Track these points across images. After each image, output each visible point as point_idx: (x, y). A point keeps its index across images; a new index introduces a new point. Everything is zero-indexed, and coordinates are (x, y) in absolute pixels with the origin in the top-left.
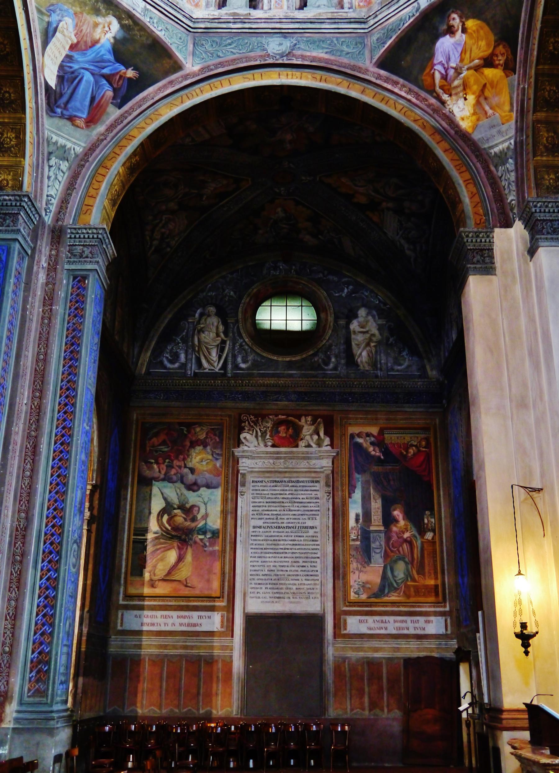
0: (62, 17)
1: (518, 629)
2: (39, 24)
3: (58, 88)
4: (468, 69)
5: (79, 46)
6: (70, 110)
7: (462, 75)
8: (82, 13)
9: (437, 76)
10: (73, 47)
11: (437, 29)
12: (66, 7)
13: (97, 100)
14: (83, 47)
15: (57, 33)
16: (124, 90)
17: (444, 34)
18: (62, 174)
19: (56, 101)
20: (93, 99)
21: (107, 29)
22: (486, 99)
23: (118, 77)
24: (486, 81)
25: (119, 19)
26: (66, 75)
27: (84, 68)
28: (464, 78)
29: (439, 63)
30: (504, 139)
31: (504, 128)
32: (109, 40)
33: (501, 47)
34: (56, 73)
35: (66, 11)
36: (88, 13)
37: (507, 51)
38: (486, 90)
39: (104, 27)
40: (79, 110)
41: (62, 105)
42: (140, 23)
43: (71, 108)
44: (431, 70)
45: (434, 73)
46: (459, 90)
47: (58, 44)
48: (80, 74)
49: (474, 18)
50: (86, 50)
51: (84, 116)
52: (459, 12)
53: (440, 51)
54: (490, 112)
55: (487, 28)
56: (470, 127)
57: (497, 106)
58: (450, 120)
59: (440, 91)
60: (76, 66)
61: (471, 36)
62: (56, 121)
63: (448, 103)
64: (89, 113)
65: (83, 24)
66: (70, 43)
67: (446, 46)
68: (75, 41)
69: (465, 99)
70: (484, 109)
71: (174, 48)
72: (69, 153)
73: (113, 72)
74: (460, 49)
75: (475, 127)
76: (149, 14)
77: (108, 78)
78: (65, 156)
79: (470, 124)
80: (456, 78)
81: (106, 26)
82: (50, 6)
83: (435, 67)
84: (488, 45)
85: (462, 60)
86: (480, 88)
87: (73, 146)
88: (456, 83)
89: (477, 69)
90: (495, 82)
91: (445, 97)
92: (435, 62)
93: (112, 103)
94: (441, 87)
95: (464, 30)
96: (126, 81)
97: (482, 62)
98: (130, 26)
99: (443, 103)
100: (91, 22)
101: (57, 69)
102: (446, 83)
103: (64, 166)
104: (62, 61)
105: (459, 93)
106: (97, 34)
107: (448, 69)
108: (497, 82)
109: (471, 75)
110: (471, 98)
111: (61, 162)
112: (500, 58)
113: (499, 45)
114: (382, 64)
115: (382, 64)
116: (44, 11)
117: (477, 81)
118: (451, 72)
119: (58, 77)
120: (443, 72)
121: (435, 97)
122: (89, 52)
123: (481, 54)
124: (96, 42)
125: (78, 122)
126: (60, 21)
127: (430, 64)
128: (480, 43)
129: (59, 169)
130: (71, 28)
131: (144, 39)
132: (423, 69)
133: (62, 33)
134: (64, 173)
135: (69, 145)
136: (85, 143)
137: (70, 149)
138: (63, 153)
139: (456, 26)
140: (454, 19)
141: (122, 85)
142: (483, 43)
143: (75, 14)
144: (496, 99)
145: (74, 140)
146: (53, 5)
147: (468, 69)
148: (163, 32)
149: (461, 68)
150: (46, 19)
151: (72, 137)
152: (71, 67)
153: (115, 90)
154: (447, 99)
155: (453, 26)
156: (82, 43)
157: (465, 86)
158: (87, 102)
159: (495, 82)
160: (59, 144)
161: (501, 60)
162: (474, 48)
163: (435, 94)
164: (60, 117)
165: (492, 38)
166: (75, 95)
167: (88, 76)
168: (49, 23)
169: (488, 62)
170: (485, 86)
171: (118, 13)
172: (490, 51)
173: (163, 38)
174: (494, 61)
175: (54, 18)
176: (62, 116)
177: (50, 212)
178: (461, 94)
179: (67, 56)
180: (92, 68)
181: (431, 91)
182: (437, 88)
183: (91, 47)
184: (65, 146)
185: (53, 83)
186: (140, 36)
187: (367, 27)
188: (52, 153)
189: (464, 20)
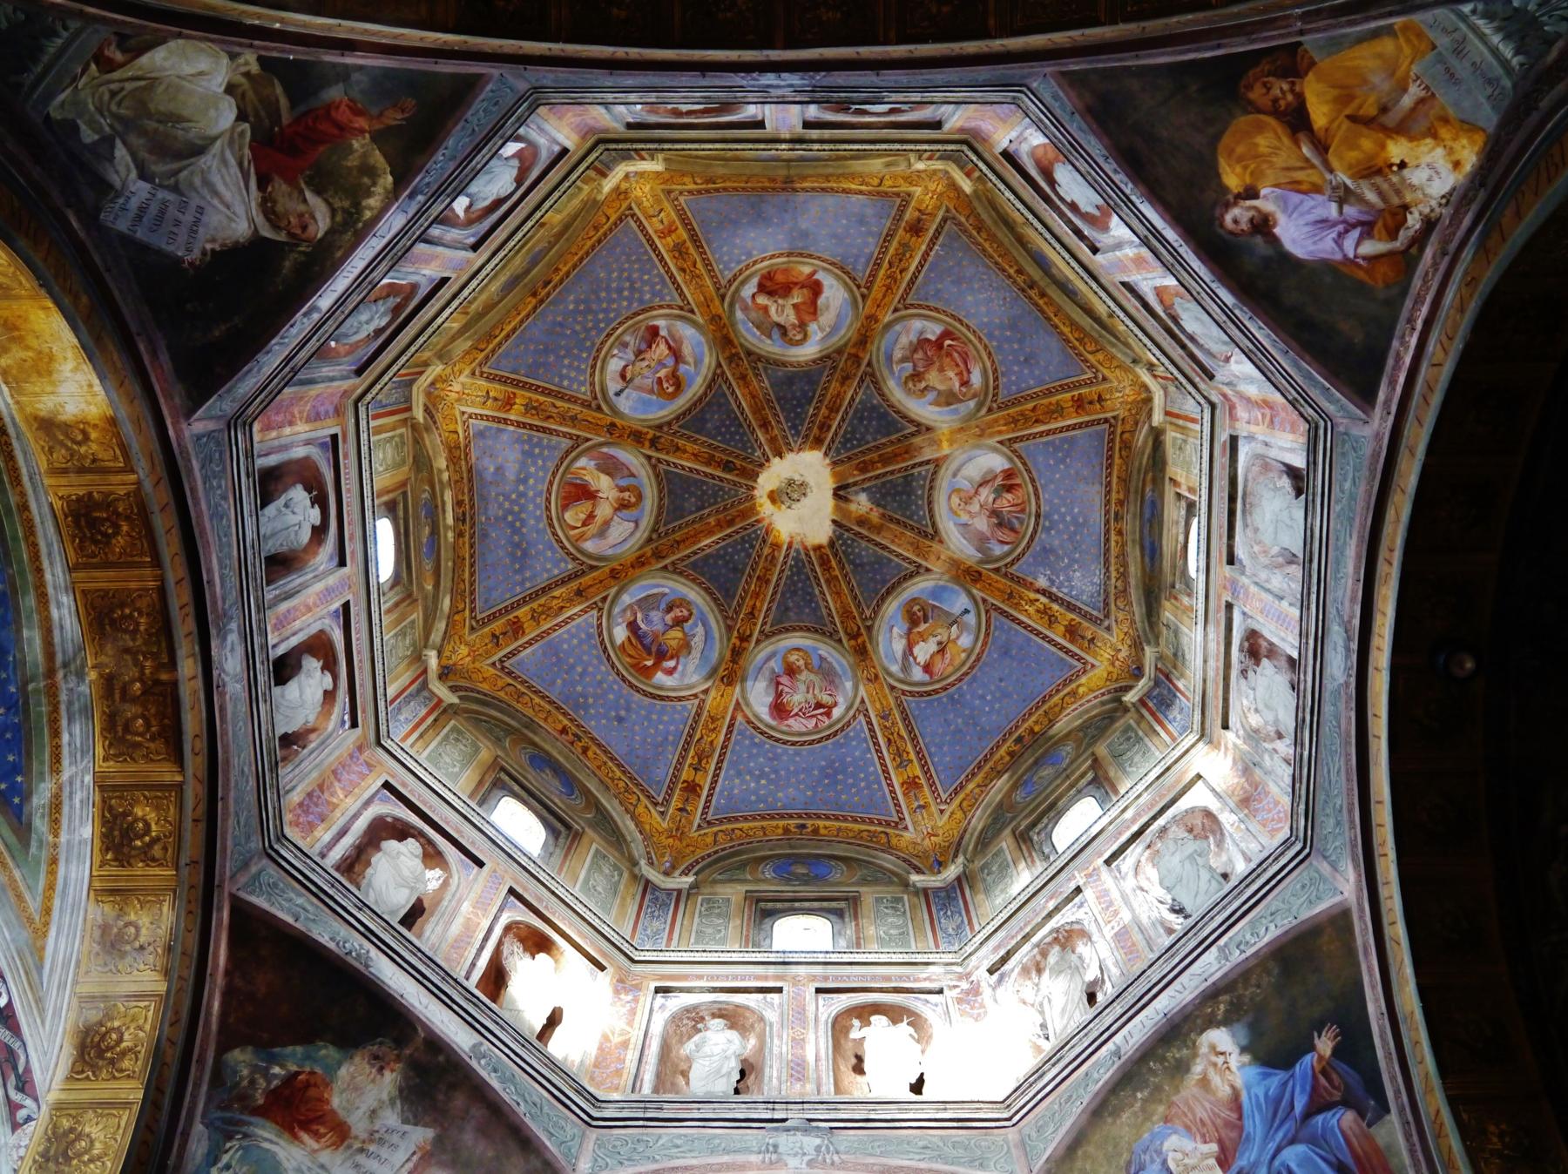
4: (1331, 171)
7: (1349, 182)
8: (1171, 1105)
9: (1370, 248)
17: (1274, 241)
21: (1220, 1060)
22: (1384, 110)
24: (1342, 118)
25: (1211, 1023)
28: (1351, 177)
29: (1340, 246)
30: (1471, 36)
31: (1443, 42)
32: (1243, 1065)
33: (1253, 95)
36: (1177, 1091)
37: (1256, 80)
38: (1361, 112)
39: (1215, 1065)
42: (1232, 976)
44: (1357, 265)
45: (1364, 258)
46: (1385, 186)
49: (1218, 176)
52: (1217, 212)
53: (1312, 248)
55: (1226, 139)
56: (1472, 142)
57: (1393, 74)
58: (1459, 200)
63: (1427, 210)
67: (1302, 230)
69: (1402, 165)
70: (1413, 110)
71: (1306, 914)
74: (1296, 198)
75: (1468, 126)
76: (1232, 946)
79: (1465, 142)
80: (1361, 200)
81: (1214, 1058)
83: (1351, 255)
84: (1260, 128)
85: (1316, 189)
86: (1365, 131)
88: (1371, 196)
89: (1322, 147)
90: (1336, 92)
91: (1414, 221)
92: (1338, 257)
94: (1392, 234)
96: (1342, 1067)
97: (1302, 136)
98: (1231, 1003)
99: (1429, 224)
100: (1195, 1090)
102: (1380, 224)
105: (1392, 185)
106: (1224, 1091)
107: (1345, 222)
108: (1333, 87)
109: (1341, 158)
110: (1396, 150)
112: (1276, 92)
113: (1250, 102)
114: (1365, 395)
115: (1365, 395)
118: (1351, 211)
120: (1355, 233)
121: (1422, 250)
123: (1286, 141)
124: (1235, 1102)
127: (1344, 269)
128: (1263, 150)
131: (1266, 979)
132: (1361, 288)
139: (1251, 213)
140: (1236, 221)
142: (1263, 142)
143: (1166, 1120)
144: (1376, 79)
147: (1331, 171)
148: (1272, 927)
149: (1334, 189)
154: (1416, 215)
155: (1251, 220)
157: (1373, 170)
159: (1336, 92)
161: (1280, 87)
162: (1280, 161)
163: (1414, 251)
165: (1243, 121)
169: (1297, 121)
170: (1353, 118)
171: (1199, 1021)
172: (1271, 121)
173: (1279, 932)
174: (1288, 105)
178: (1395, 179)
181: (1405, 261)
182: (1397, 245)
186: (1258, 986)
187: (1322, 423)
189: (1231, 198)
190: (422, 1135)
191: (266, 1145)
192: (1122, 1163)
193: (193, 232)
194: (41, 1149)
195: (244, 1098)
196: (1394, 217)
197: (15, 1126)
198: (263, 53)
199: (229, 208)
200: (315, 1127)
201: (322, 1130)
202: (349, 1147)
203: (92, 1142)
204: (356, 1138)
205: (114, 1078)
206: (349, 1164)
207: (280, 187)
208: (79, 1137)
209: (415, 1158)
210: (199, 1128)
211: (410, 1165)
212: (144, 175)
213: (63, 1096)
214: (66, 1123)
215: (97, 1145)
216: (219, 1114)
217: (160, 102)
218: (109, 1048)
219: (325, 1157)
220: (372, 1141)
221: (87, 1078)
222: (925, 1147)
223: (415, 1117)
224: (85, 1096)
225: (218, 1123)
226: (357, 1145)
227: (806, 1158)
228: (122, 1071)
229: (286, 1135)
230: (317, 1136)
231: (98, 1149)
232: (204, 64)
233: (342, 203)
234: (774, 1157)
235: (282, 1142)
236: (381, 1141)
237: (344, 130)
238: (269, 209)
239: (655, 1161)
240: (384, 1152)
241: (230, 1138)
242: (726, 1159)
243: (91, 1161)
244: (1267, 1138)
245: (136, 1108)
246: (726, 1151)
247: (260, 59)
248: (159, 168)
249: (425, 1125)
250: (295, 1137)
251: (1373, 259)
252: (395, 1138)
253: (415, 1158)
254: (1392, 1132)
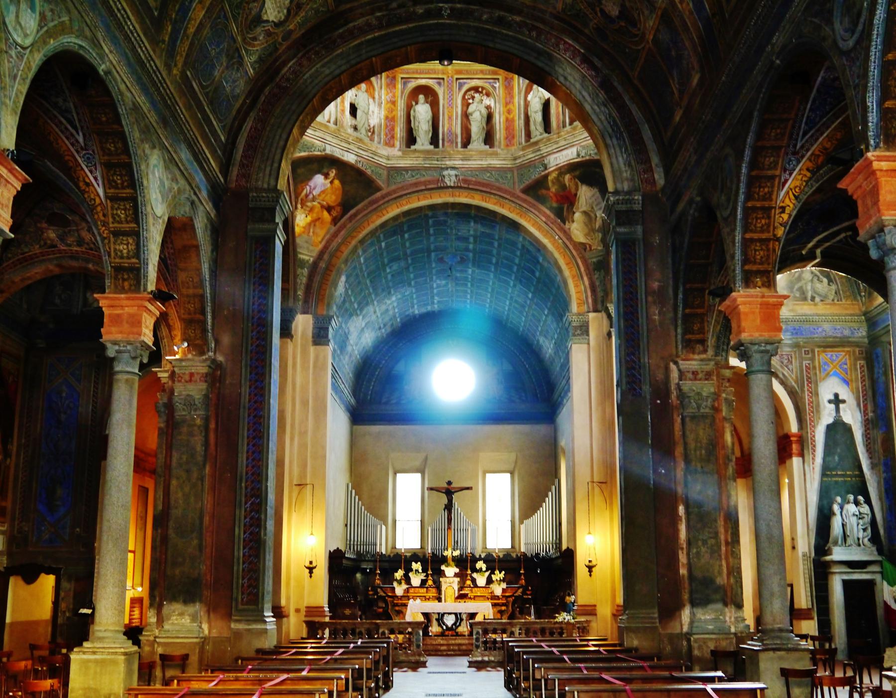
1: (308, 564)
9: (305, 192)
11: (323, 168)
31: (311, 248)
54: (311, 234)
55: (341, 191)
59: (300, 201)
61: (332, 188)
67: (319, 180)
74: (323, 189)
75: (300, 235)
84: (335, 201)
85: (319, 195)
88: (309, 204)
89: (322, 207)
91: (299, 206)
94: (302, 200)
95: (331, 182)
99: (296, 208)
110: (309, 219)
117: (318, 213)
118: (311, 196)
142: (334, 197)
157: (311, 210)
161: (334, 213)
165: (339, 200)
169: (329, 209)
193: (593, 196)
196: (303, 205)
198: (562, 224)
199: (585, 194)
207: (573, 191)
212: (596, 217)
217: (586, 231)
232: (575, 232)
233: (561, 179)
237: (555, 195)
238: (577, 189)
247: (565, 224)
248: (593, 215)
251: (303, 190)
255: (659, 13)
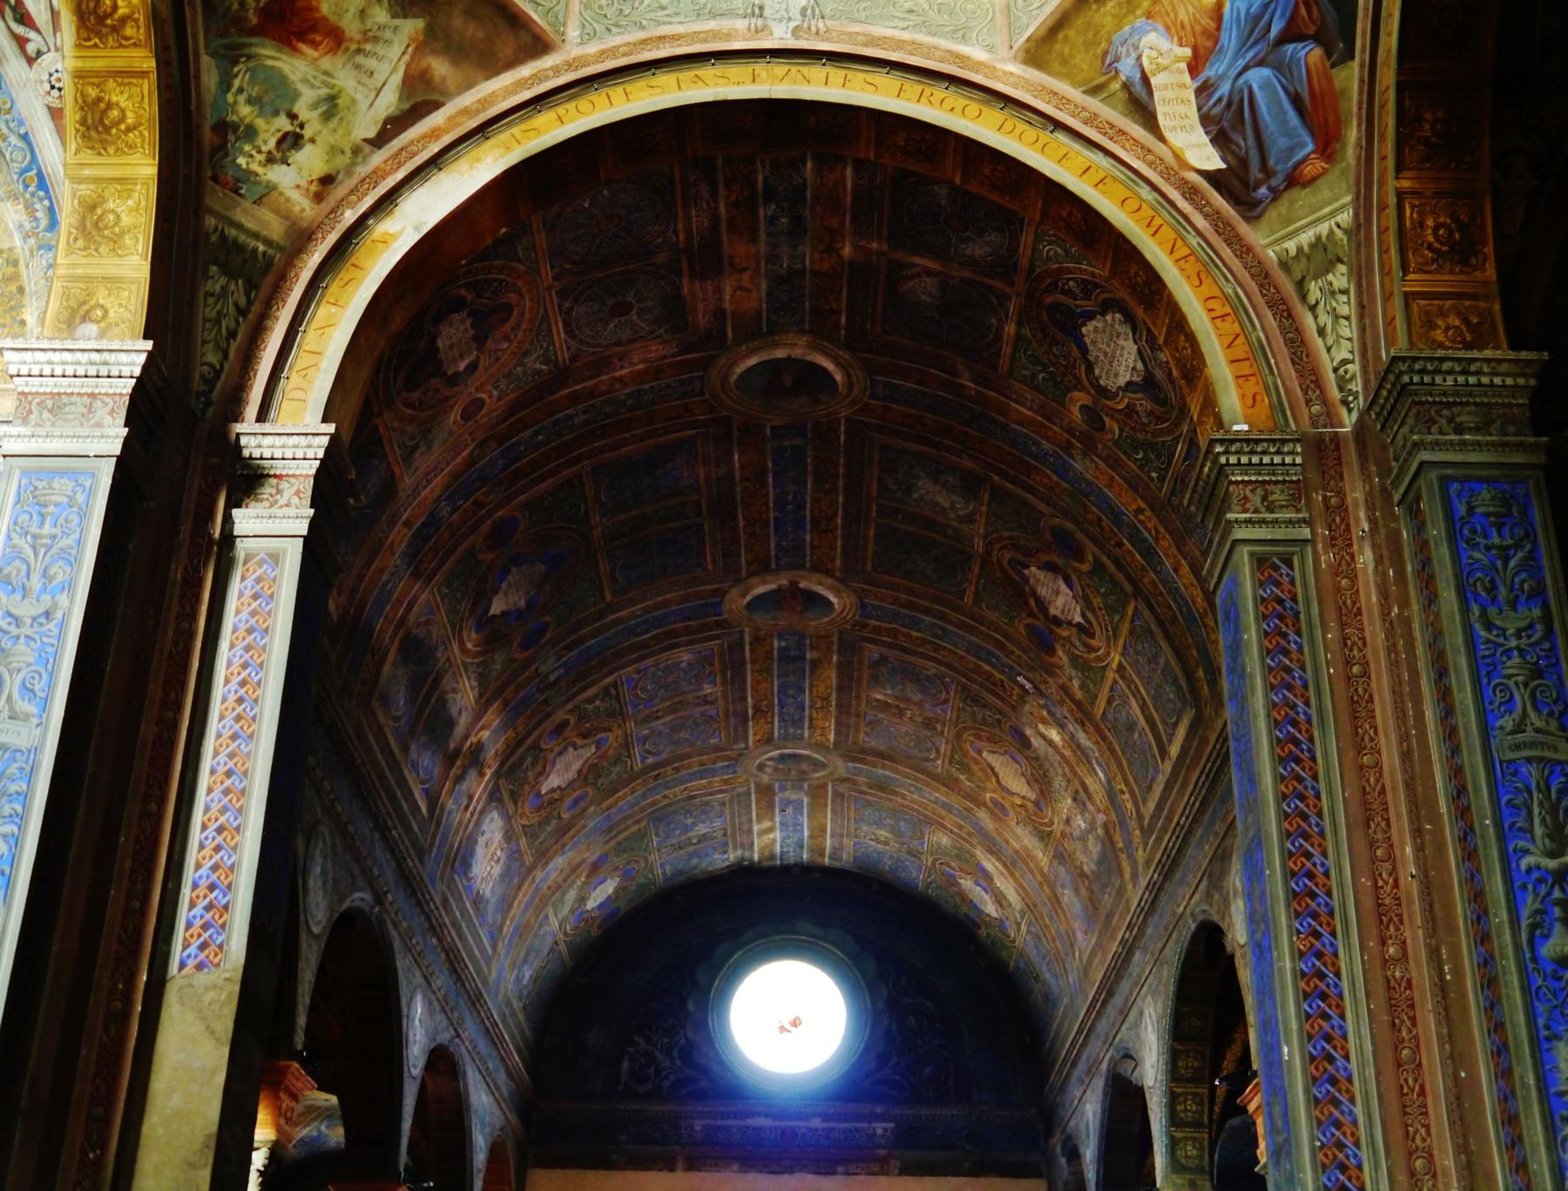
0: (1136, 48)
2: (1114, 108)
3: (1230, 158)
5: (1201, 50)
6: (1279, 168)
10: (1194, 68)
12: (1127, 28)
13: (1305, 95)
14: (1209, 44)
15: (1153, 81)
16: (1332, 17)
18: (1344, 298)
19: (1245, 182)
20: (1296, 101)
23: (1303, 10)
26: (1227, 121)
27: (1240, 74)
34: (1206, 139)
35: (1134, 30)
40: (1291, 150)
41: (1260, 176)
43: (1277, 163)
47: (1170, 94)
48: (1241, 91)
50: (1217, 40)
51: (1310, 147)
60: (1225, 89)
62: (1272, 214)
64: (1312, 133)
65: (1174, 10)
66: (1183, 66)
68: (1188, 52)
72: (1335, 244)
73: (1288, 14)
77: (1291, 34)
78: (1330, 256)
82: (1103, 62)
87: (1333, 222)
93: (1333, 66)
101: (1201, 131)
103: (1339, 278)
104: (1199, 110)
111: (1330, 277)
116: (1103, 79)
119: (1215, 141)
122: (1224, 35)
125: (1308, 170)
126: (1139, 58)
129: (1333, 293)
130: (1164, 44)
133: (1161, 69)
134: (1344, 292)
135: (1323, 229)
136: (1349, 191)
137: (1331, 232)
138: (1322, 256)
141: (1320, 12)
145: (1327, 210)
146: (1105, 53)
150: (1116, 86)
151: (1321, 208)
152: (1220, 100)
153: (1318, 39)
156: (1199, 39)
158: (1293, 119)
160: (1306, 248)
164: (1274, 200)
166: (1265, 135)
167: (1257, 76)
168: (1126, 86)
175: (1127, 68)
176: (1276, 194)
177: (1356, 398)
179: (1199, 91)
180: (1251, 54)
183: (1218, 28)
184: (1319, 238)
185: (1212, 160)
188: (1303, 278)
190: (412, 27)
191: (270, 62)
192: (1099, 51)
194: (78, 117)
195: (238, 22)
197: (30, 61)
200: (311, 37)
201: (319, 38)
202: (347, 49)
203: (123, 111)
204: (351, 40)
205: (121, 46)
206: (350, 66)
208: (109, 106)
209: (410, 50)
210: (206, 60)
211: (407, 58)
213: (80, 64)
214: (93, 93)
215: (129, 114)
216: (219, 42)
218: (107, 15)
219: (326, 63)
220: (366, 40)
221: (96, 45)
222: (910, 11)
223: (403, 9)
224: (100, 64)
225: (222, 51)
226: (354, 47)
227: (792, 25)
228: (127, 39)
229: (286, 49)
230: (315, 45)
231: (131, 119)
234: (760, 22)
235: (284, 57)
236: (375, 39)
239: (643, 28)
240: (380, 49)
241: (235, 62)
242: (711, 25)
243: (128, 130)
244: (1238, 54)
245: (154, 77)
246: (714, 15)
249: (414, 16)
250: (295, 49)
252: (388, 34)
253: (410, 50)
254: (1350, 77)
255: (397, 471)
